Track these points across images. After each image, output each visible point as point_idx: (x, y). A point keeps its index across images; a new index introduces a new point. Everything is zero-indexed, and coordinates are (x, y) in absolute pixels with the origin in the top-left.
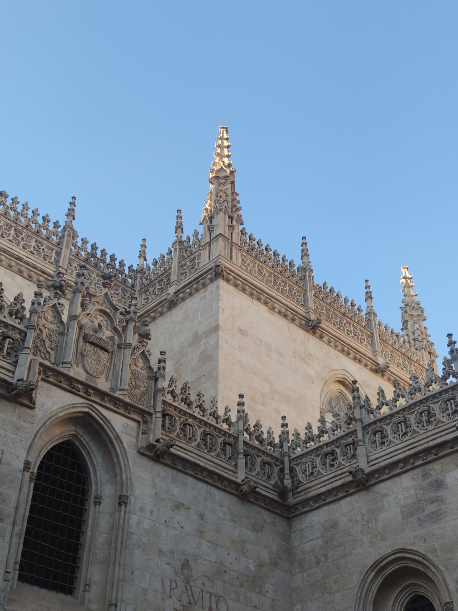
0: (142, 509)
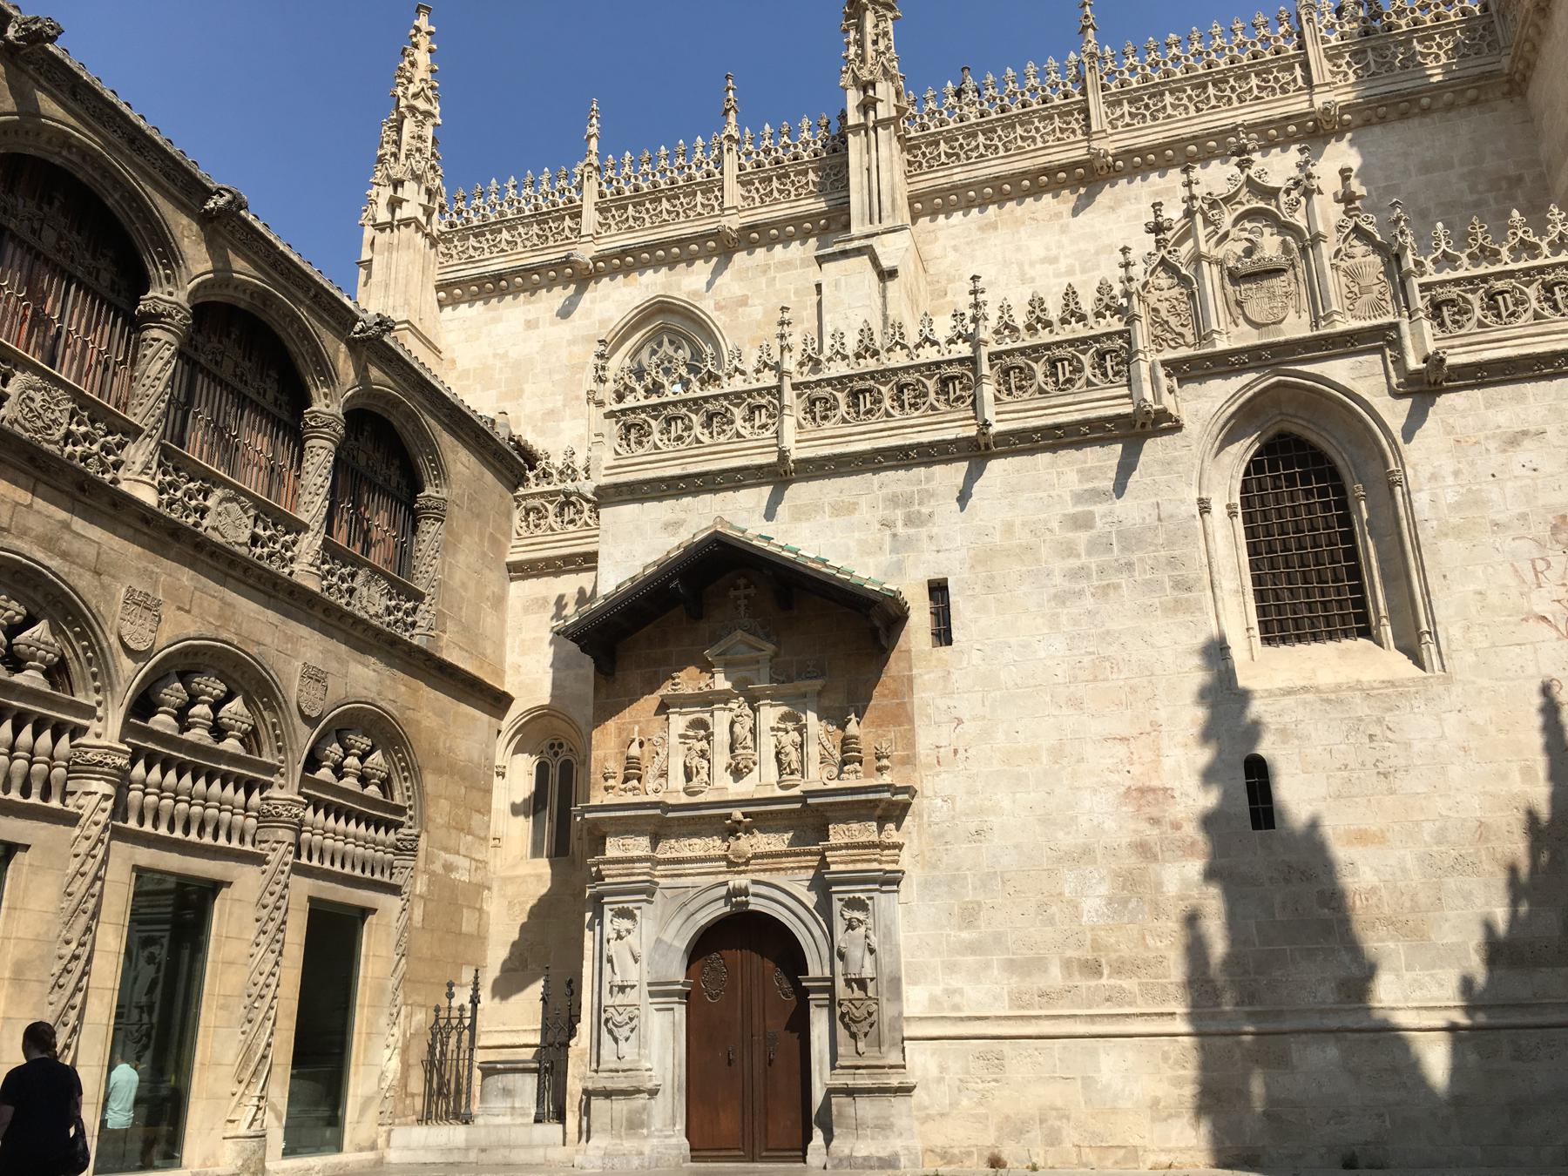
0: (1433, 477)
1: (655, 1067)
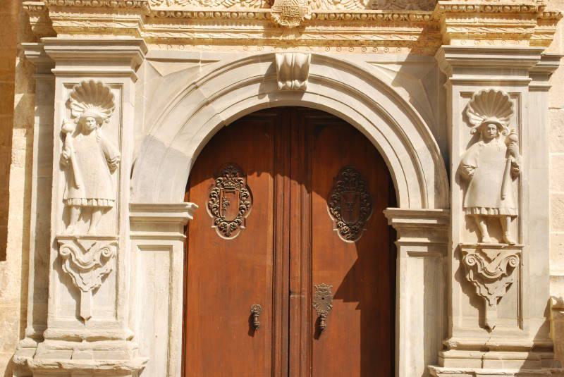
1: (138, 334)
